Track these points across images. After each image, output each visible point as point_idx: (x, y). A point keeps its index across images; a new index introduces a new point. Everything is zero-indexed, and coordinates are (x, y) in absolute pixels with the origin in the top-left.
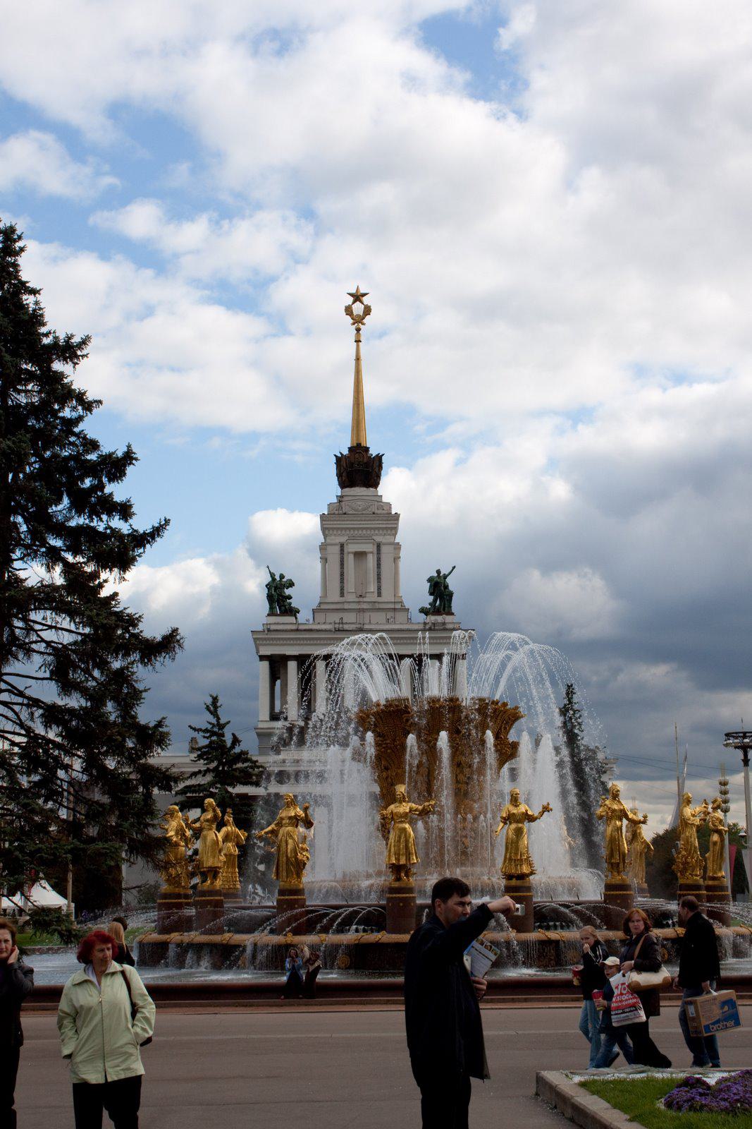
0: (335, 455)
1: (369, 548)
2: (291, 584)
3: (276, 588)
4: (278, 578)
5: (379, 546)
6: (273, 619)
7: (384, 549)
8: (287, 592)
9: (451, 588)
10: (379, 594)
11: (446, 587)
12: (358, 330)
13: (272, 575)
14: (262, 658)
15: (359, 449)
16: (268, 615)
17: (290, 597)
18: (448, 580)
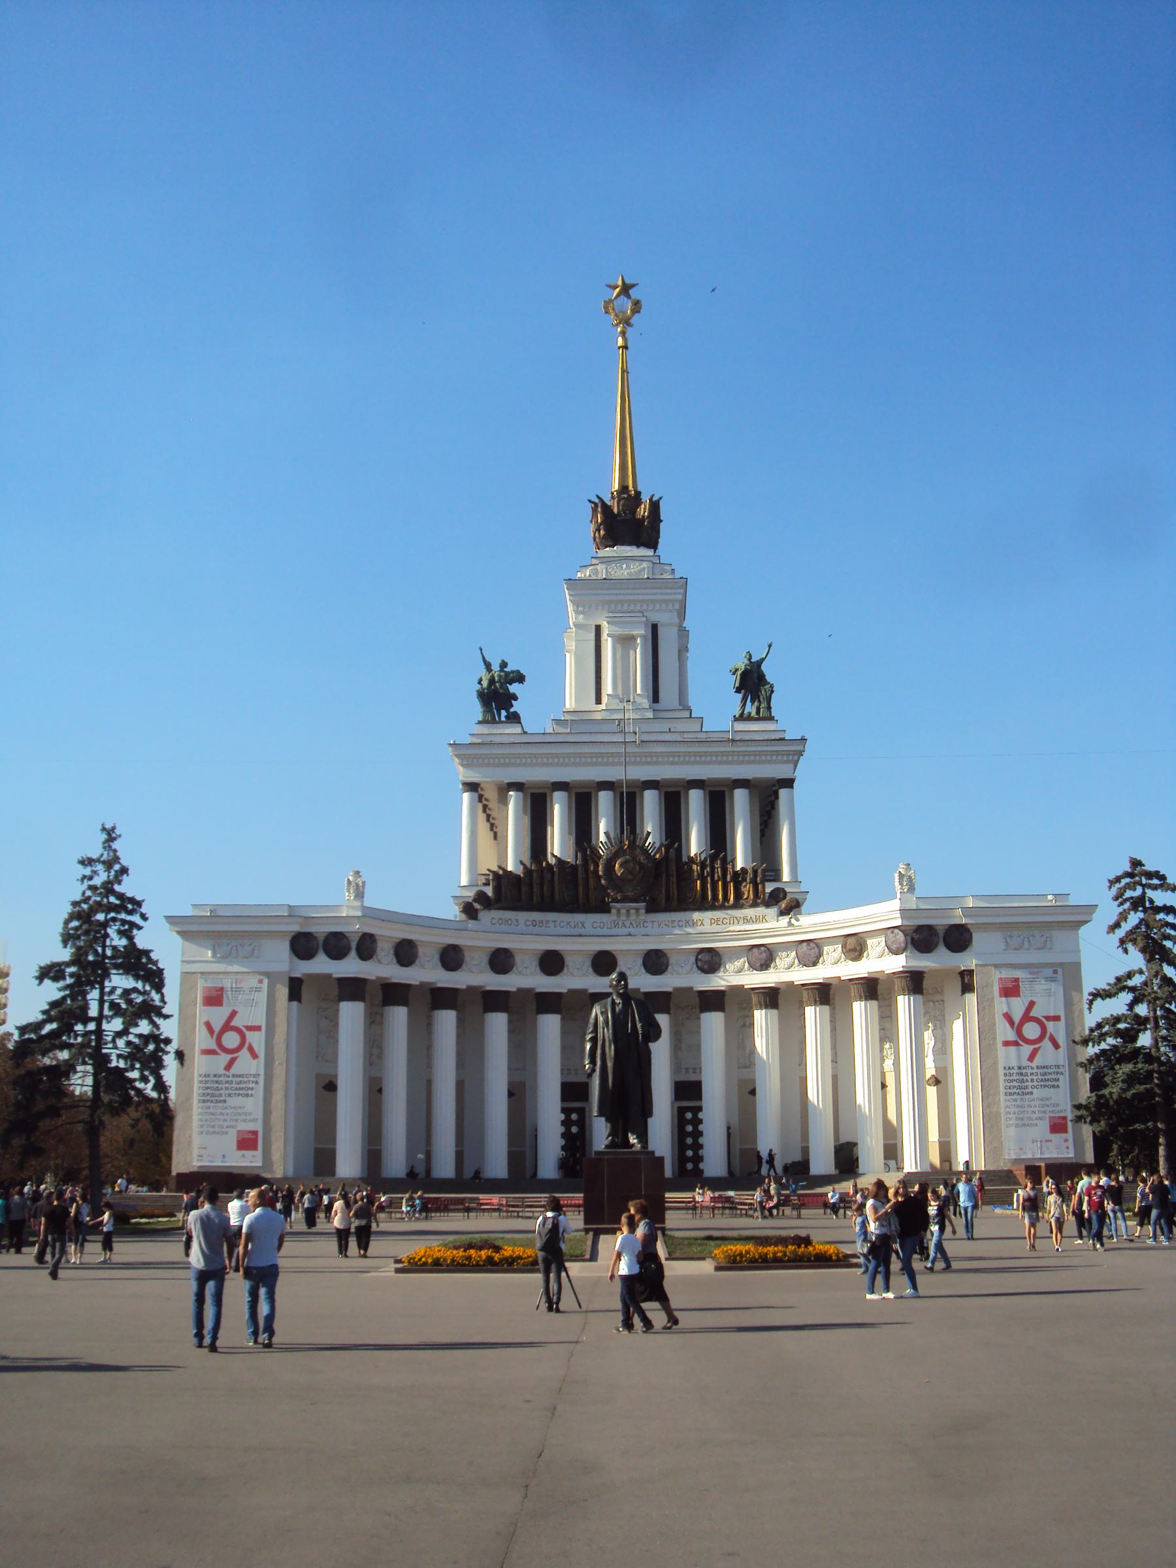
0: (590, 501)
1: (640, 631)
2: (520, 678)
3: (492, 681)
4: (496, 667)
5: (655, 628)
7: (661, 632)
8: (514, 688)
9: (768, 678)
10: (656, 698)
11: (762, 679)
12: (623, 333)
13: (488, 666)
16: (480, 722)
17: (516, 698)
18: (764, 667)
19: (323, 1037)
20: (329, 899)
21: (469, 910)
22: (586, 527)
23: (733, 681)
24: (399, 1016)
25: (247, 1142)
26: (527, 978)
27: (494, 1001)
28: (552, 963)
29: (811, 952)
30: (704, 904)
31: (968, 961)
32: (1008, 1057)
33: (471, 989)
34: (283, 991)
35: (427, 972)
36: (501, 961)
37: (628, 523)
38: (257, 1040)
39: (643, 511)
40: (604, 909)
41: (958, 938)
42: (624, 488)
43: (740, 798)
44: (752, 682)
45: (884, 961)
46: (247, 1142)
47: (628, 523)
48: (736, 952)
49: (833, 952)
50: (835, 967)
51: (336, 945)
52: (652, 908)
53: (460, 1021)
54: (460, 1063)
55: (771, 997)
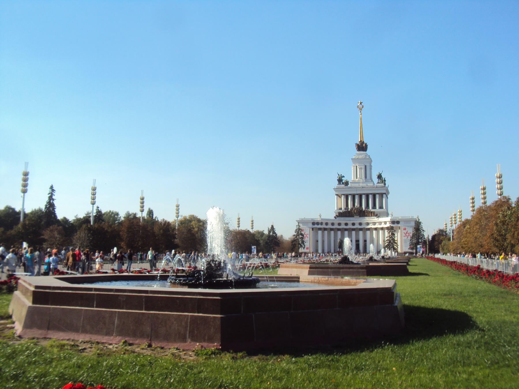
2: (344, 177)
6: (339, 186)
8: (343, 179)
14: (337, 195)
15: (362, 142)
19: (316, 235)
20: (317, 218)
21: (335, 217)
22: (355, 148)
23: (377, 177)
24: (326, 232)
25: (307, 248)
26: (343, 226)
27: (339, 230)
28: (346, 224)
29: (380, 223)
30: (367, 216)
31: (399, 225)
32: (403, 238)
33: (336, 228)
34: (311, 230)
35: (330, 226)
36: (339, 224)
37: (362, 147)
38: (308, 236)
39: (364, 145)
40: (353, 216)
41: (398, 222)
42: (361, 141)
43: (377, 196)
44: (380, 177)
45: (388, 225)
46: (307, 248)
47: (362, 147)
48: (371, 223)
49: (383, 223)
50: (383, 225)
51: (318, 224)
52: (360, 216)
53: (334, 233)
54: (334, 237)
55: (376, 229)
